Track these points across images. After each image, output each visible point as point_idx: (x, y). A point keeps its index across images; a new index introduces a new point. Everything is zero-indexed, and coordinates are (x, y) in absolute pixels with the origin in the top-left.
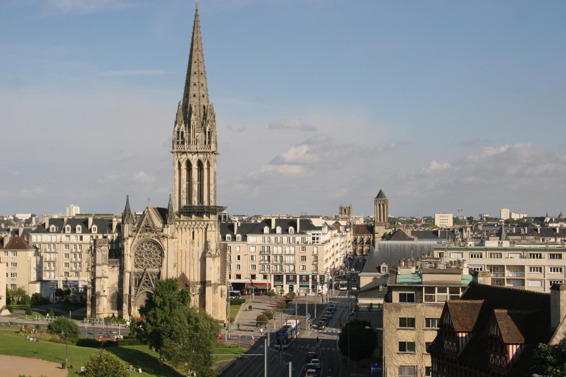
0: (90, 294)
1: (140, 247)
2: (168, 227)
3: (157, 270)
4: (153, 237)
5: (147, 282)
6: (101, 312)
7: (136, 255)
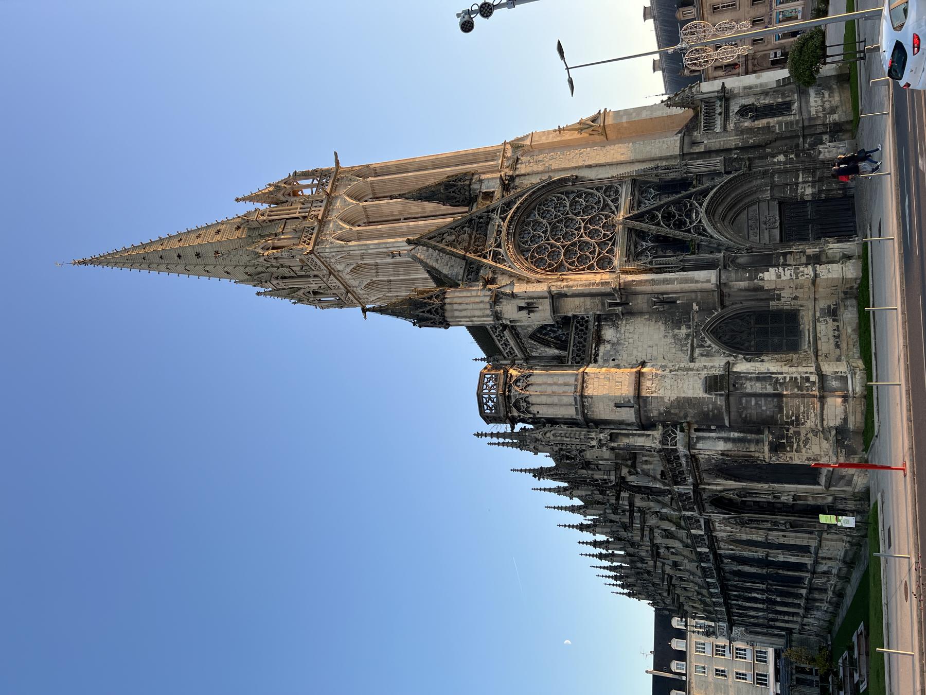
0: (719, 438)
1: (532, 257)
2: (481, 181)
3: (625, 199)
4: (504, 219)
5: (668, 217)
6: (811, 373)
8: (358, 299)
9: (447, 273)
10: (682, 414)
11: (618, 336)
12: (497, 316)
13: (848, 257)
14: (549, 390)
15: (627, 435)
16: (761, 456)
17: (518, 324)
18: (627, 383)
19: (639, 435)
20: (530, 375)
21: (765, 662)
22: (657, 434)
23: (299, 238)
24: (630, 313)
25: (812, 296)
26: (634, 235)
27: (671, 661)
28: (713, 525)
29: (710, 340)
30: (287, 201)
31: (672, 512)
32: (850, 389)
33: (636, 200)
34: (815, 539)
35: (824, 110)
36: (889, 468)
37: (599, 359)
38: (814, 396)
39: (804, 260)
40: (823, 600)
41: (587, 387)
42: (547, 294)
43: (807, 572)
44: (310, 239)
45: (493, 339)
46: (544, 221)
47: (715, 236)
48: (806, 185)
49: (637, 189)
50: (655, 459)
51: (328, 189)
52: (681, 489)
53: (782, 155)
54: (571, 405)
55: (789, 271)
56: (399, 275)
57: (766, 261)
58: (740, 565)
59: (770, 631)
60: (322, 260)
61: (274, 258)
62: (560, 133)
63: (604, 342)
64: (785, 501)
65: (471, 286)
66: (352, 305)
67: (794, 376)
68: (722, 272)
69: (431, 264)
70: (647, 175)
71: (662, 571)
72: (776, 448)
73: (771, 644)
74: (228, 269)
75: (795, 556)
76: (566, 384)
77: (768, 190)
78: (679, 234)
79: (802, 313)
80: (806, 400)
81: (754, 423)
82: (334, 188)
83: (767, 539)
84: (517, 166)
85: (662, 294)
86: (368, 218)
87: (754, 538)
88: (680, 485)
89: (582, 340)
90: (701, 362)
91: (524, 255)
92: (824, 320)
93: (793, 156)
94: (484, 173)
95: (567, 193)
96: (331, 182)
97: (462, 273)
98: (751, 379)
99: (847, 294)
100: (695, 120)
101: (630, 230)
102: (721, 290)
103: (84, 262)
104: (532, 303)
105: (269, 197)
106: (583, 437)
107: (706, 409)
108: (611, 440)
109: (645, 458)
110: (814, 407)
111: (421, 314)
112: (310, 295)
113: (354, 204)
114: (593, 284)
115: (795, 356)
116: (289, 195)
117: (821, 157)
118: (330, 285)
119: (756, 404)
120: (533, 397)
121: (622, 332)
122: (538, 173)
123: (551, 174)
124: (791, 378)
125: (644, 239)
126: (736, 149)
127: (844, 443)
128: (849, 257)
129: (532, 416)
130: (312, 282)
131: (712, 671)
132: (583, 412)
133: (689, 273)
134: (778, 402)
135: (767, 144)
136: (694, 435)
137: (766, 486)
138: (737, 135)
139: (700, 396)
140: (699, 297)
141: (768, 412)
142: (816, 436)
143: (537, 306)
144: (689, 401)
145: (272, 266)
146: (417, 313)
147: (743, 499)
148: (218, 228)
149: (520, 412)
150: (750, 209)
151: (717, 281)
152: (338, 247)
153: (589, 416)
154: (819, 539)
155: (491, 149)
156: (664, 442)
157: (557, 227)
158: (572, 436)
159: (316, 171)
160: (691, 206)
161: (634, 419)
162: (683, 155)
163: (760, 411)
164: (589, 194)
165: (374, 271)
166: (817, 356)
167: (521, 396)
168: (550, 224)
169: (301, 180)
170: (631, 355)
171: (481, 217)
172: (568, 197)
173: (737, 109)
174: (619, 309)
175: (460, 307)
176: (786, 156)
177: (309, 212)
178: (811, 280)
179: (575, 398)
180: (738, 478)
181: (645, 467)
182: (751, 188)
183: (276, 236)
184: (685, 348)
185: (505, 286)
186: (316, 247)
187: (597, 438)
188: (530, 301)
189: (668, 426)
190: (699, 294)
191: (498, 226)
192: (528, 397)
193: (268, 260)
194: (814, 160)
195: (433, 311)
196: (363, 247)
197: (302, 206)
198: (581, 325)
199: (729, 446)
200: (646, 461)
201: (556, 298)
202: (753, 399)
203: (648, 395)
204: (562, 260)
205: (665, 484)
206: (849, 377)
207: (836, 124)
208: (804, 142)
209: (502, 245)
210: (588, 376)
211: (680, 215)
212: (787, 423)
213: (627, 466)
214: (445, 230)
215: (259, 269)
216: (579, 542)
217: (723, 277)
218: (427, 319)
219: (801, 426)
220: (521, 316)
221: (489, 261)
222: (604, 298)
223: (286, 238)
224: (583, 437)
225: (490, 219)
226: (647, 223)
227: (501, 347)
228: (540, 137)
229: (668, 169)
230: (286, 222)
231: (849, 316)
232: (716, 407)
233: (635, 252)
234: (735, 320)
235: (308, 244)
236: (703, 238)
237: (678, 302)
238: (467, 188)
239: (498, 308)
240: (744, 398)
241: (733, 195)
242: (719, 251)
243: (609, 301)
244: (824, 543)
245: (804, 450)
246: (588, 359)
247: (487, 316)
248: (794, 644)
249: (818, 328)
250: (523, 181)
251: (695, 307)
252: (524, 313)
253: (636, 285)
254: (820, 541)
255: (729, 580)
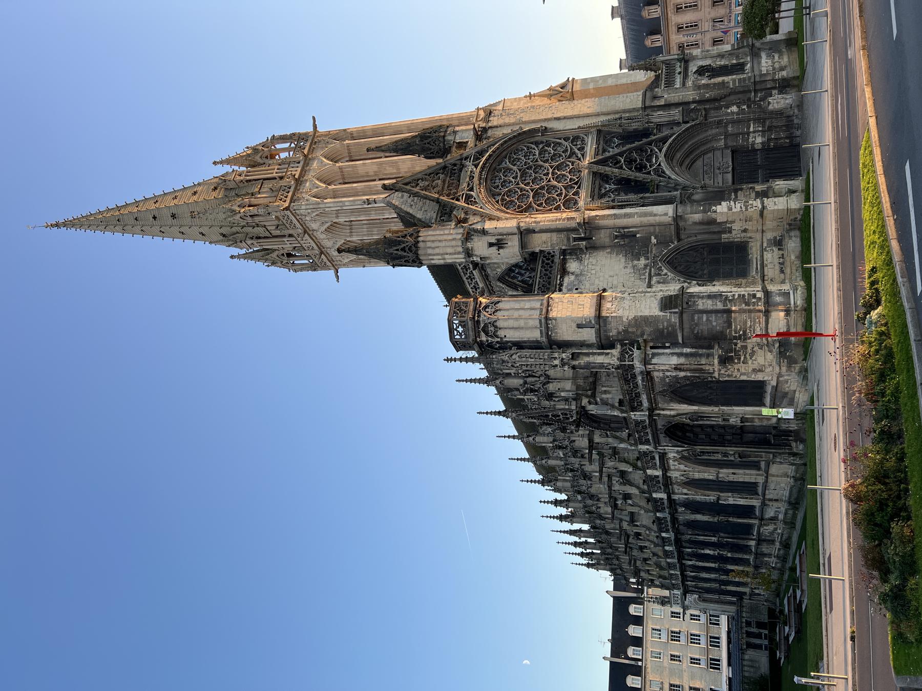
0: (673, 354)
1: (503, 200)
2: (455, 132)
4: (476, 166)
5: (630, 161)
6: (758, 291)
7: (528, 209)
8: (331, 261)
9: (420, 217)
10: (639, 333)
11: (581, 268)
12: (468, 253)
13: (791, 192)
14: (516, 314)
15: (587, 354)
16: (711, 368)
17: (488, 262)
18: (588, 305)
19: (599, 354)
20: (499, 302)
21: (719, 647)
22: (616, 352)
23: (276, 197)
24: (593, 247)
25: (760, 228)
26: (599, 178)
27: (628, 647)
28: (668, 463)
29: (667, 269)
30: (264, 164)
31: (629, 447)
32: (792, 302)
33: (601, 148)
34: (762, 475)
35: (774, 69)
36: (821, 335)
37: (564, 288)
38: (760, 311)
39: (753, 195)
40: (771, 555)
41: (551, 310)
42: (516, 231)
43: (756, 518)
44: (286, 197)
45: (463, 281)
46: (515, 168)
47: (673, 177)
48: (757, 135)
49: (602, 139)
50: (614, 389)
51: (306, 151)
52: (636, 416)
53: (735, 106)
54: (536, 327)
55: (739, 204)
56: (372, 235)
57: (719, 196)
58: (693, 514)
59: (722, 597)
60: (298, 217)
61: (251, 216)
62: (530, 99)
63: (568, 274)
64: (734, 423)
65: (444, 226)
66: (325, 267)
67: (742, 293)
68: (678, 206)
69: (405, 209)
70: (611, 125)
71: (620, 527)
72: (725, 361)
73: (722, 611)
74: (204, 230)
75: (744, 498)
76: (532, 309)
77: (722, 139)
78: (640, 176)
79: (751, 244)
80: (753, 315)
81: (705, 338)
82: (311, 150)
83: (718, 477)
84: (490, 119)
85: (624, 228)
86: (344, 178)
87: (706, 476)
88: (636, 411)
89: (547, 272)
90: (657, 288)
91: (495, 199)
92: (771, 250)
93: (745, 107)
94: (458, 126)
95: (537, 144)
96: (308, 144)
97: (435, 217)
98: (703, 297)
99: (791, 226)
100: (656, 83)
101: (593, 173)
102: (677, 224)
103: (57, 225)
104: (502, 240)
105: (246, 159)
106: (546, 357)
107: (661, 327)
108: (573, 358)
109: (604, 389)
110: (759, 321)
111: (396, 252)
112: (284, 258)
113: (330, 164)
114: (560, 220)
115: (744, 281)
116: (267, 157)
117: (771, 107)
118: (304, 245)
119: (707, 319)
120: (501, 321)
121: (586, 264)
122: (510, 125)
123: (522, 126)
124: (739, 295)
125: (607, 182)
126: (694, 102)
127: (786, 354)
128: (794, 192)
129: (499, 340)
130: (286, 242)
131: (667, 656)
132: (547, 333)
133: (648, 207)
134: (727, 317)
135: (721, 98)
136: (650, 352)
137: (716, 409)
138: (694, 90)
139: (656, 314)
140: (657, 230)
141: (718, 328)
142: (761, 349)
143: (506, 242)
144: (646, 320)
145: (248, 225)
146: (391, 251)
147: (695, 422)
148: (195, 190)
149: (488, 336)
150: (706, 157)
151: (673, 214)
152: (313, 204)
153: (553, 338)
154: (765, 475)
155: (464, 115)
156: (620, 359)
157: (527, 173)
158: (536, 356)
159: (294, 134)
160: (651, 151)
161: (594, 339)
162: (645, 108)
163: (710, 326)
164: (558, 143)
165: (348, 231)
166: (763, 280)
167: (489, 321)
168: (520, 170)
169: (278, 143)
170: (593, 284)
171: (455, 165)
172: (537, 147)
173: (695, 69)
174: (584, 243)
175: (433, 245)
176: (738, 107)
177: (286, 172)
178: (759, 212)
179: (540, 320)
180: (691, 401)
181: (604, 396)
182: (707, 137)
183: (252, 195)
184: (643, 277)
185: (477, 223)
186: (292, 204)
187: (559, 358)
188: (500, 237)
189: (626, 344)
190: (657, 228)
191: (471, 172)
192: (496, 321)
193: (245, 218)
194: (764, 111)
195: (407, 249)
196: (338, 204)
197: (279, 167)
198: (548, 259)
199: (682, 360)
200: (605, 391)
201: (524, 234)
202: (705, 315)
203: (608, 315)
204: (531, 202)
205: (623, 412)
206: (791, 292)
207: (784, 80)
208: (755, 96)
209: (475, 188)
210: (553, 300)
211: (642, 160)
212: (735, 338)
213: (587, 396)
214: (420, 176)
215: (234, 229)
216: (541, 502)
217: (680, 210)
218: (401, 257)
219: (748, 341)
220: (492, 252)
221: (462, 203)
222: (569, 233)
223: (263, 197)
224: (546, 357)
225: (463, 166)
226: (611, 167)
227: (470, 290)
228: (511, 103)
229: (631, 119)
230: (262, 183)
231: (793, 245)
232: (671, 325)
233: (599, 194)
234: (690, 252)
235: (285, 201)
236: (662, 179)
237: (638, 236)
238: (441, 139)
239: (469, 245)
240: (697, 315)
241: (690, 143)
242: (677, 190)
243: (574, 236)
244: (770, 479)
245: (750, 362)
246: (553, 288)
247: (459, 253)
248: (744, 610)
249: (765, 257)
250: (496, 133)
251: (654, 240)
252: (494, 249)
253: (599, 219)
254: (767, 477)
255: (683, 534)
